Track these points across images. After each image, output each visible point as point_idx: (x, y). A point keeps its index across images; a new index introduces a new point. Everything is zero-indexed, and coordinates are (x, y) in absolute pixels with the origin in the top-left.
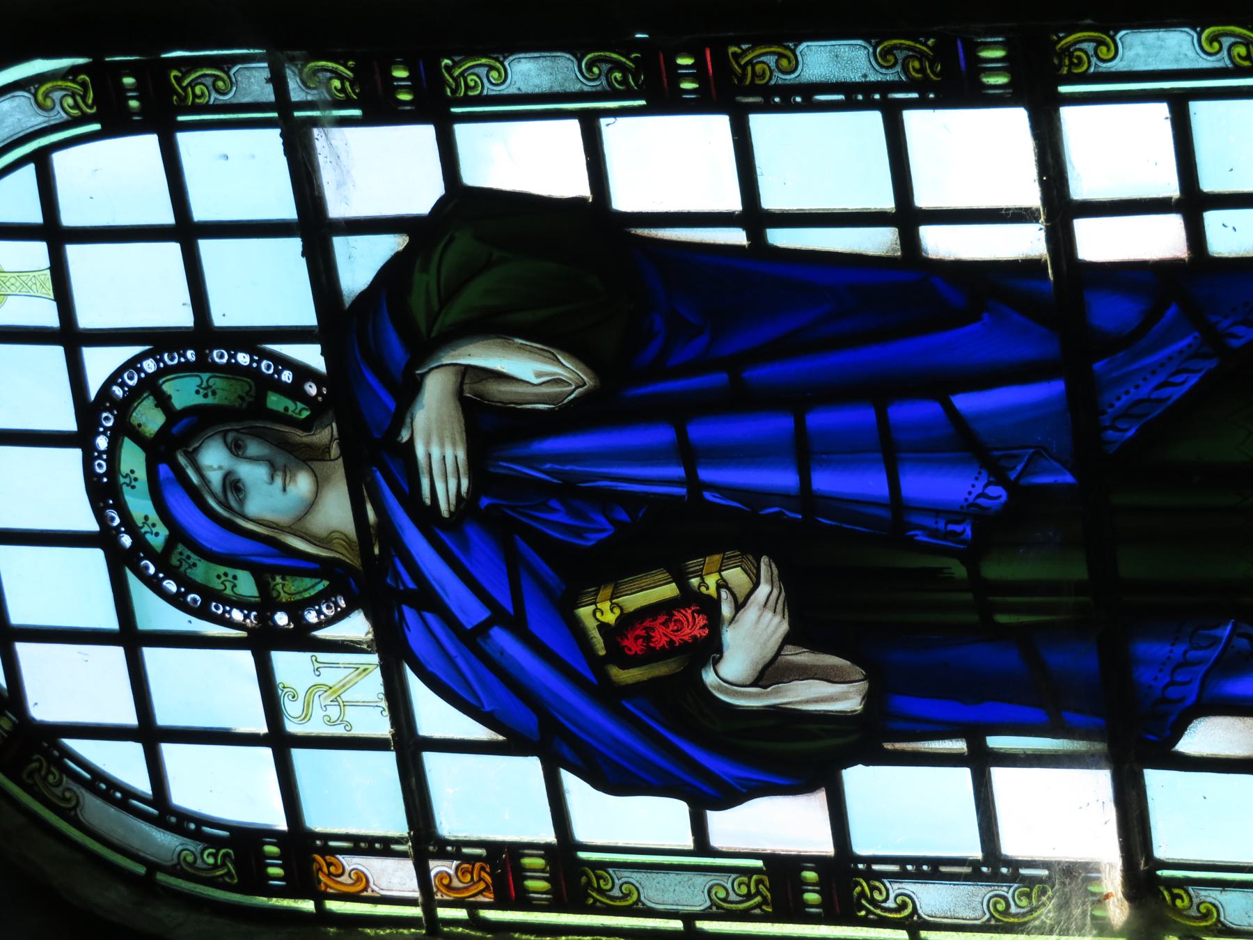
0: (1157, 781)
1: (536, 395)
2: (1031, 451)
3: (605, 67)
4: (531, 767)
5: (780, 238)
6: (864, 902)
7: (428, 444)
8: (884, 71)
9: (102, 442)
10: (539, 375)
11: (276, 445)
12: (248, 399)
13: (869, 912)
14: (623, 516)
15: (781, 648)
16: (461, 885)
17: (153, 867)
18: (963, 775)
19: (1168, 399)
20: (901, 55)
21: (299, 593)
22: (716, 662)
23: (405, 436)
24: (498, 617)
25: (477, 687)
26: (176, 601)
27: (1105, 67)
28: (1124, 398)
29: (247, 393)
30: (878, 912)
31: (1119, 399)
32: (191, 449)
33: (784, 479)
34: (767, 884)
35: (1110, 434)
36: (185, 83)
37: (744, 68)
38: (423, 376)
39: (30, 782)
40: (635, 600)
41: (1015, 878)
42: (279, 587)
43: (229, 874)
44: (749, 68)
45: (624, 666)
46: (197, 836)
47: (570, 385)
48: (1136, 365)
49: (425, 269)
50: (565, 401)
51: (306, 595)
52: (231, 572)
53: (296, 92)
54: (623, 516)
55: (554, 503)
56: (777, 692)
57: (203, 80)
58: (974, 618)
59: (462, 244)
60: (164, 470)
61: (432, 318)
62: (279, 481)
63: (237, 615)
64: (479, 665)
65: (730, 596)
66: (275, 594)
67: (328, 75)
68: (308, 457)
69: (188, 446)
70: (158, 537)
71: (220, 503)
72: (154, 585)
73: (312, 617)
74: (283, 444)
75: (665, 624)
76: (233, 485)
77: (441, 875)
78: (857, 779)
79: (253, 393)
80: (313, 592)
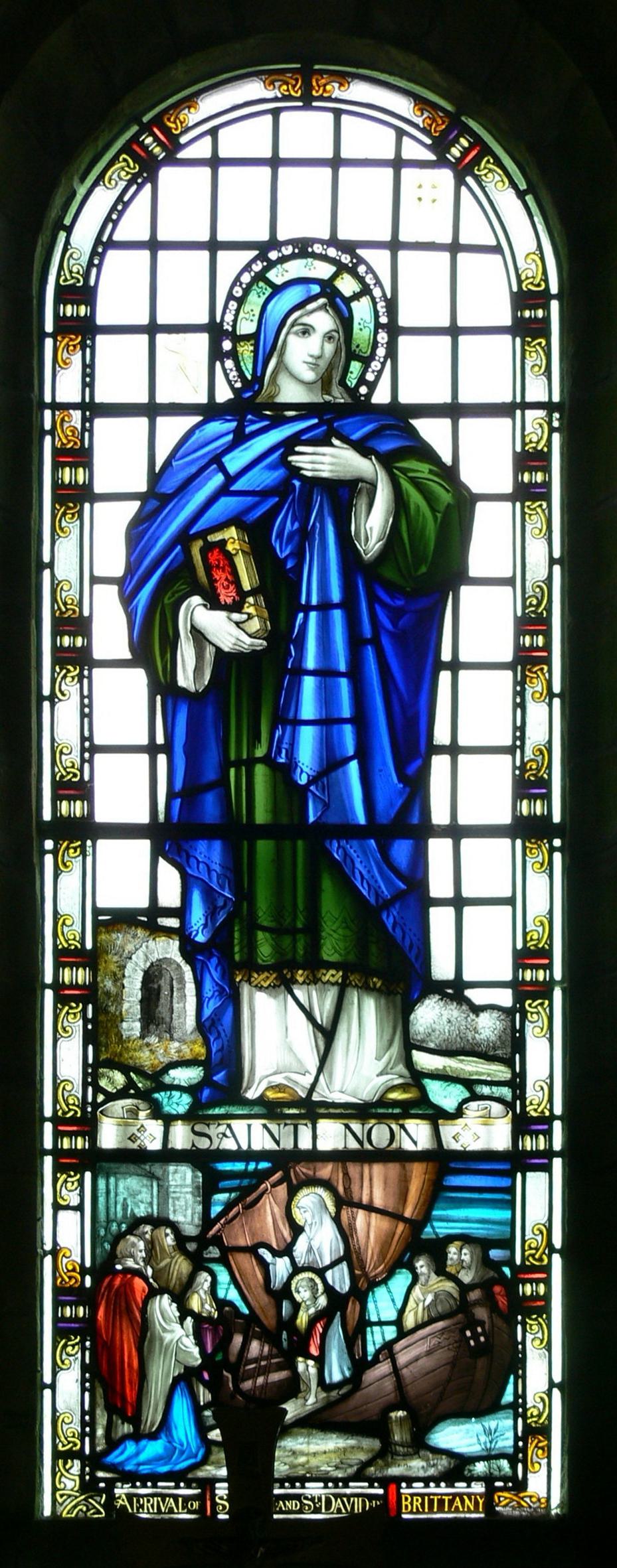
0: (143, 847)
1: (360, 525)
2: (327, 800)
3: (539, 596)
4: (142, 487)
5: (445, 677)
6: (64, 671)
7: (333, 456)
8: (531, 749)
9: (332, 252)
10: (371, 529)
11: (331, 363)
12: (357, 350)
13: (59, 674)
14: (289, 565)
15: (214, 645)
16: (65, 428)
17: (69, 230)
18: (145, 741)
19: (355, 879)
20: (539, 758)
21: (243, 360)
22: (205, 606)
23: (336, 442)
24: (230, 479)
25: (187, 459)
26: (237, 281)
27: (529, 865)
28: (355, 855)
29: (360, 350)
30: (59, 679)
31: (355, 851)
32: (328, 308)
33: (310, 663)
34: (73, 616)
35: (335, 844)
36: (538, 347)
37: (536, 672)
38: (371, 459)
39: (121, 159)
40: (240, 562)
41: (83, 760)
42: (246, 347)
43: (66, 280)
44: (535, 676)
45: (202, 550)
46: (90, 264)
47: (365, 545)
48: (373, 863)
49: (431, 472)
50: (356, 542)
51: (242, 364)
52: (256, 319)
53: (531, 414)
54: (289, 565)
55: (296, 525)
56: (188, 638)
57: (539, 359)
58: (233, 756)
59: (445, 497)
60: (316, 289)
61: (404, 471)
62: (310, 360)
63: (229, 317)
64: (202, 462)
65: (243, 620)
66: (242, 344)
67: (540, 435)
68: (325, 383)
69: (330, 306)
70: (277, 276)
71: (296, 320)
72: (247, 268)
73: (229, 364)
74: (331, 367)
75: (226, 579)
76: (307, 331)
77: (70, 416)
78: (138, 678)
79: (361, 354)
80: (244, 368)
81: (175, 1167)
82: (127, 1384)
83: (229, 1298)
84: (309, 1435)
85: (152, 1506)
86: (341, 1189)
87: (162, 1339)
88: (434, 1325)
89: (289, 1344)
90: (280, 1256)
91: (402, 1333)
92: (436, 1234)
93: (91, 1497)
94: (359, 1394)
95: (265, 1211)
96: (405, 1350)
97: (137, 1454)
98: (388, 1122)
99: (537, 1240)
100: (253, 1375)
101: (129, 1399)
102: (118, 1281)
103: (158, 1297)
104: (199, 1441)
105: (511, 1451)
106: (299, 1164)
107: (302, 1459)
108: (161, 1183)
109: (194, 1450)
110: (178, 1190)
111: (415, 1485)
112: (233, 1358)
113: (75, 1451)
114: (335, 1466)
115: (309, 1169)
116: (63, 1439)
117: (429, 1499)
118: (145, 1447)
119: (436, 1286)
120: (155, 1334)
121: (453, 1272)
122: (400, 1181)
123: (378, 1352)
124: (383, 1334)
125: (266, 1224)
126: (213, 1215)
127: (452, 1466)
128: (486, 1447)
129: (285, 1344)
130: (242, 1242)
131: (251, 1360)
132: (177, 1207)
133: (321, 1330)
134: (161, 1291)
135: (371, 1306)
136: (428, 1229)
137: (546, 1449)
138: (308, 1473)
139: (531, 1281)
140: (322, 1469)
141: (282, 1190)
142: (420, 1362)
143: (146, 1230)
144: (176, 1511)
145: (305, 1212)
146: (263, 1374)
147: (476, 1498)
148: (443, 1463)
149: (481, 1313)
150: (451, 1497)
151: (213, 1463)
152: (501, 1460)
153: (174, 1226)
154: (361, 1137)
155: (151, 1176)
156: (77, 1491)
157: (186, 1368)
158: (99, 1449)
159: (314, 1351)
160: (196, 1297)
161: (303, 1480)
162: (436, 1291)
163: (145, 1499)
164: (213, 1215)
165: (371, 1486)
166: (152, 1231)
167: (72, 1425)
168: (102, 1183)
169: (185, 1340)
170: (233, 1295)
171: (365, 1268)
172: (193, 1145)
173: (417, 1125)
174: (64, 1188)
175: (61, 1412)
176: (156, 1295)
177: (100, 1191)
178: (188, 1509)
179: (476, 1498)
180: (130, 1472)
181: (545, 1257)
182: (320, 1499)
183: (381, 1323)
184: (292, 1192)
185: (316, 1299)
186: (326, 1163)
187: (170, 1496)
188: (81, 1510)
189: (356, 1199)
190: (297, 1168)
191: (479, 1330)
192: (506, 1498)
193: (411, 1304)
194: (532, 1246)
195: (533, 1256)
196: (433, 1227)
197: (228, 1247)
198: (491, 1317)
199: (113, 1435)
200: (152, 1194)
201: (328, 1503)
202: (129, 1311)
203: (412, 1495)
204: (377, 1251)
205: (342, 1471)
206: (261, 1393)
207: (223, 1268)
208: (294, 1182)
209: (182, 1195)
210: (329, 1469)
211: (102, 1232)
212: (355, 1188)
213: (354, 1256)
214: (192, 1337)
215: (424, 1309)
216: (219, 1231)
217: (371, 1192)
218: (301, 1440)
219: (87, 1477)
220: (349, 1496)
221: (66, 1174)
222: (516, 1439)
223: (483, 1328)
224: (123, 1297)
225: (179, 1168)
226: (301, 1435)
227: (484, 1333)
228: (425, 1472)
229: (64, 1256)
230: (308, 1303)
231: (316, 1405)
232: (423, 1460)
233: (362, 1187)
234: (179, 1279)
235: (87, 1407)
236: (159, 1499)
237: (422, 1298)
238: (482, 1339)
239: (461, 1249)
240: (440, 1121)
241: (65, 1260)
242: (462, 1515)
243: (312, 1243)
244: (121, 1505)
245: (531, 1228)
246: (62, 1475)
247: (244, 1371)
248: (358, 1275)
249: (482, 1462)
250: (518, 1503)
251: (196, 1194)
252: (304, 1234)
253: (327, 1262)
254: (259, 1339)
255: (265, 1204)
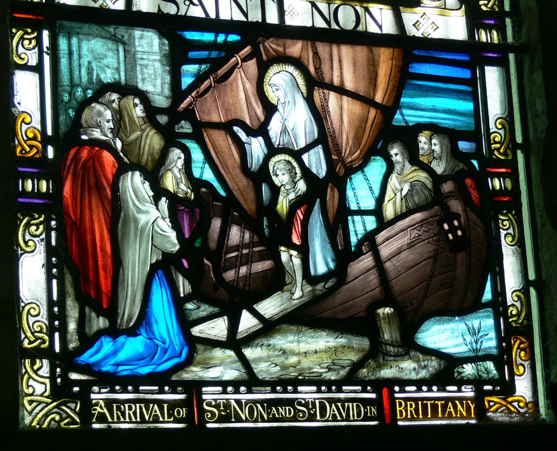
81: (141, 33)
82: (102, 272)
83: (205, 177)
84: (299, 332)
85: (135, 413)
86: (312, 69)
87: (136, 221)
88: (412, 217)
89: (270, 231)
90: (255, 136)
91: (382, 224)
92: (406, 122)
93: (65, 404)
94: (345, 288)
95: (237, 86)
96: (387, 242)
97: (115, 352)
98: (353, 4)
99: (500, 134)
100: (235, 264)
101: (103, 289)
102: (85, 153)
103: (130, 173)
104: (182, 337)
105: (495, 352)
106: (268, 39)
107: (293, 360)
108: (127, 48)
109: (177, 348)
110: (145, 57)
111: (408, 388)
112: (213, 245)
113: (43, 348)
114: (327, 368)
115: (278, 45)
116: (29, 334)
117: (422, 404)
118: (124, 344)
119: (410, 176)
120: (129, 213)
121: (426, 161)
122: (369, 65)
123: (360, 242)
124: (364, 223)
125: (239, 100)
126: (184, 86)
127: (442, 367)
128: (472, 348)
129: (266, 231)
130: (215, 118)
131: (232, 247)
132: (146, 76)
133: (302, 217)
134: (134, 167)
135: (349, 193)
136: (398, 116)
137: (528, 350)
138: (300, 375)
139: (499, 175)
140: (314, 370)
141: (252, 65)
142: (403, 255)
143: (112, 99)
144: (161, 419)
145: (277, 90)
146: (246, 264)
147: (467, 403)
148: (434, 364)
149: (456, 206)
150: (443, 402)
151: (199, 363)
152: (488, 362)
153: (144, 97)
154: (327, 17)
155: (117, 40)
156: (47, 397)
157: (164, 254)
158: (72, 346)
159: (296, 240)
160: (169, 175)
161: (296, 383)
162: (412, 180)
163: (127, 405)
164: (184, 86)
165: (364, 391)
166: (120, 99)
167: (39, 318)
168: (63, 43)
169: (160, 222)
170: (209, 176)
171: (341, 154)
172: (159, 9)
173: (381, 9)
174: (20, 46)
175: (26, 302)
176: (128, 172)
177: (62, 52)
178: (175, 417)
179: (467, 403)
180: (107, 372)
181: (509, 151)
182: (314, 404)
183: (361, 212)
184: (263, 69)
185: (296, 183)
186: (295, 41)
187: (155, 401)
188: (53, 419)
189: (327, 80)
190: (266, 43)
191: (456, 223)
192: (496, 403)
193: (389, 194)
194: (496, 139)
195: (498, 150)
196: (402, 114)
197: (201, 121)
198: (465, 211)
199: (87, 330)
200: (118, 59)
201: (323, 409)
202: (99, 188)
203: (406, 400)
204: (351, 136)
205: (334, 373)
206: (245, 285)
207: (196, 145)
208: (264, 57)
209: (151, 63)
210: (322, 370)
211: (66, 98)
212: (325, 68)
213: (329, 139)
214: (168, 220)
215: (402, 200)
216: (191, 103)
217: (341, 73)
218: (291, 338)
219: (59, 380)
220: (343, 401)
221: (23, 30)
222: (500, 339)
223: (459, 222)
224: (91, 171)
225: (145, 33)
226: (291, 332)
227: (460, 227)
228: (417, 374)
229: (23, 121)
230: (287, 187)
231: (303, 299)
232: (414, 361)
233: (332, 67)
234: (151, 154)
235: (55, 297)
236: (142, 405)
237: (400, 188)
238: (459, 233)
239: (431, 139)
240: (401, 8)
241: (25, 127)
242: (453, 422)
243: (286, 123)
244: (99, 412)
245: (494, 121)
246: (30, 377)
247: (225, 259)
248: (336, 160)
249: (469, 364)
250: (508, 409)
251: (165, 62)
252: (277, 113)
253: (302, 145)
254: (239, 225)
255: (236, 79)
